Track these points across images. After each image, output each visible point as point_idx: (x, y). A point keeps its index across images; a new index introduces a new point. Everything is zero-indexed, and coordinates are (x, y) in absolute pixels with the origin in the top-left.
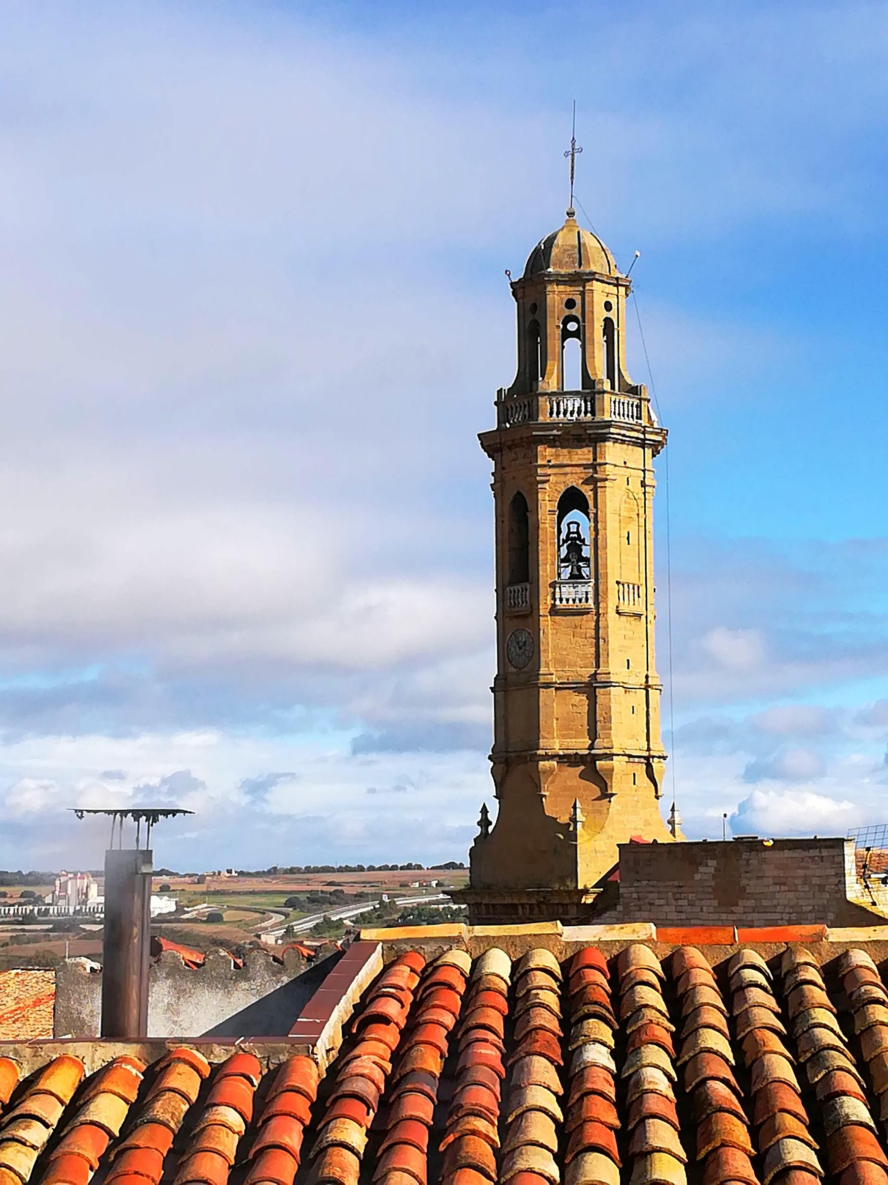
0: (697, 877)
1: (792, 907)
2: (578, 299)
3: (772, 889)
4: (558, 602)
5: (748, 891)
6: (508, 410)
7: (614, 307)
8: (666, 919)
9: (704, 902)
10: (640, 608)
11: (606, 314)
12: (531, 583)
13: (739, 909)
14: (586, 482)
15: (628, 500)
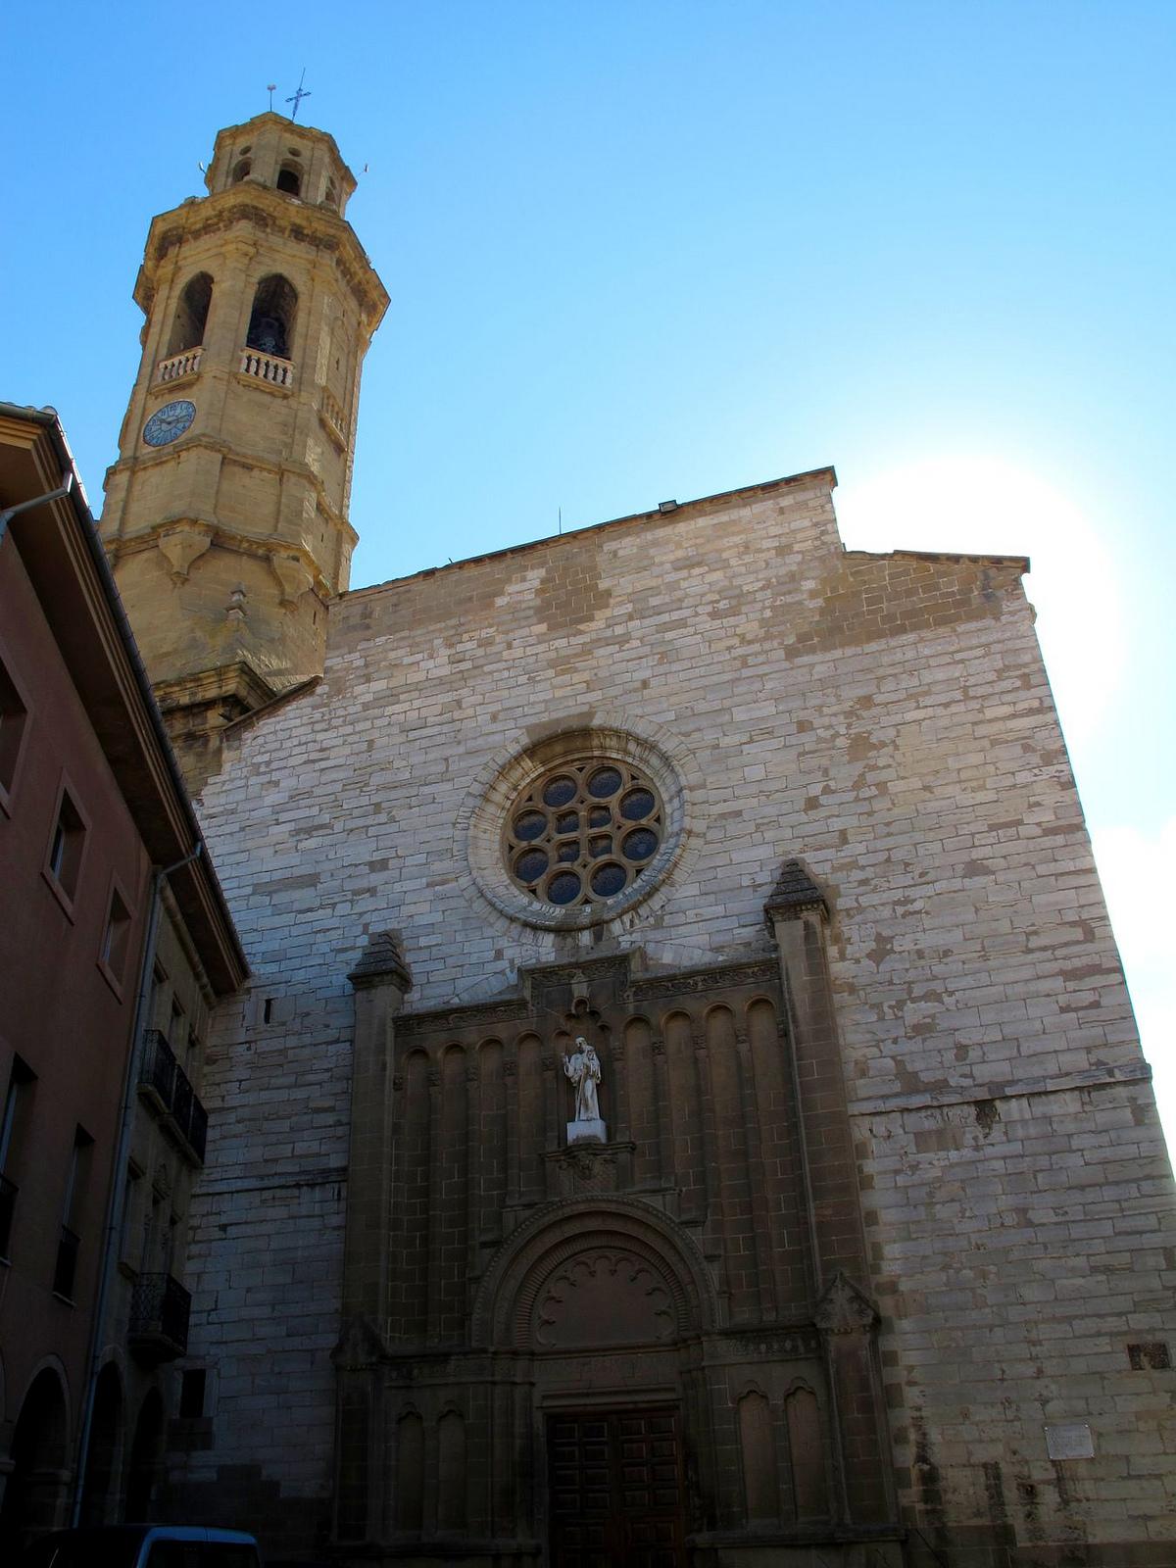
0: (500, 601)
1: (719, 593)
3: (670, 578)
5: (614, 594)
8: (427, 679)
9: (511, 636)
12: (204, 350)
13: (598, 623)
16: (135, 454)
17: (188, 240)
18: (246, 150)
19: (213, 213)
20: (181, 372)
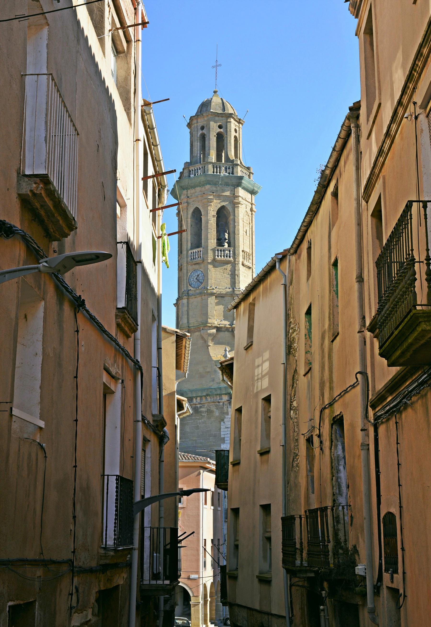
4: (217, 257)
6: (190, 171)
7: (238, 132)
10: (250, 265)
11: (235, 134)
12: (203, 248)
15: (246, 215)
18: (202, 128)
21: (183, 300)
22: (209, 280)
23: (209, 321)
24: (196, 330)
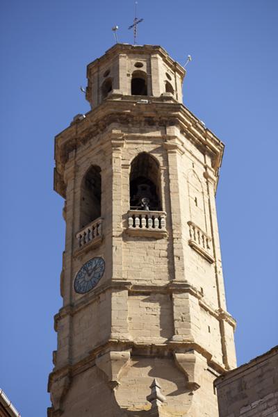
2: (145, 64)
12: (103, 219)
14: (156, 150)
16: (71, 301)
17: (80, 146)
18: (107, 73)
19: (92, 124)
20: (91, 237)
21: (62, 321)
22: (114, 265)
23: (114, 335)
24: (87, 366)
